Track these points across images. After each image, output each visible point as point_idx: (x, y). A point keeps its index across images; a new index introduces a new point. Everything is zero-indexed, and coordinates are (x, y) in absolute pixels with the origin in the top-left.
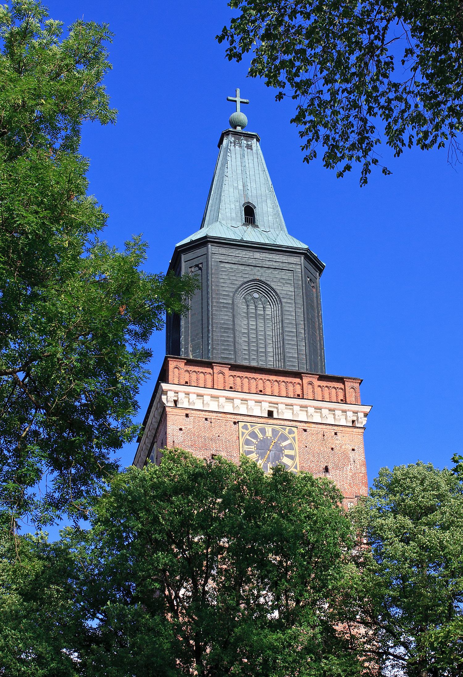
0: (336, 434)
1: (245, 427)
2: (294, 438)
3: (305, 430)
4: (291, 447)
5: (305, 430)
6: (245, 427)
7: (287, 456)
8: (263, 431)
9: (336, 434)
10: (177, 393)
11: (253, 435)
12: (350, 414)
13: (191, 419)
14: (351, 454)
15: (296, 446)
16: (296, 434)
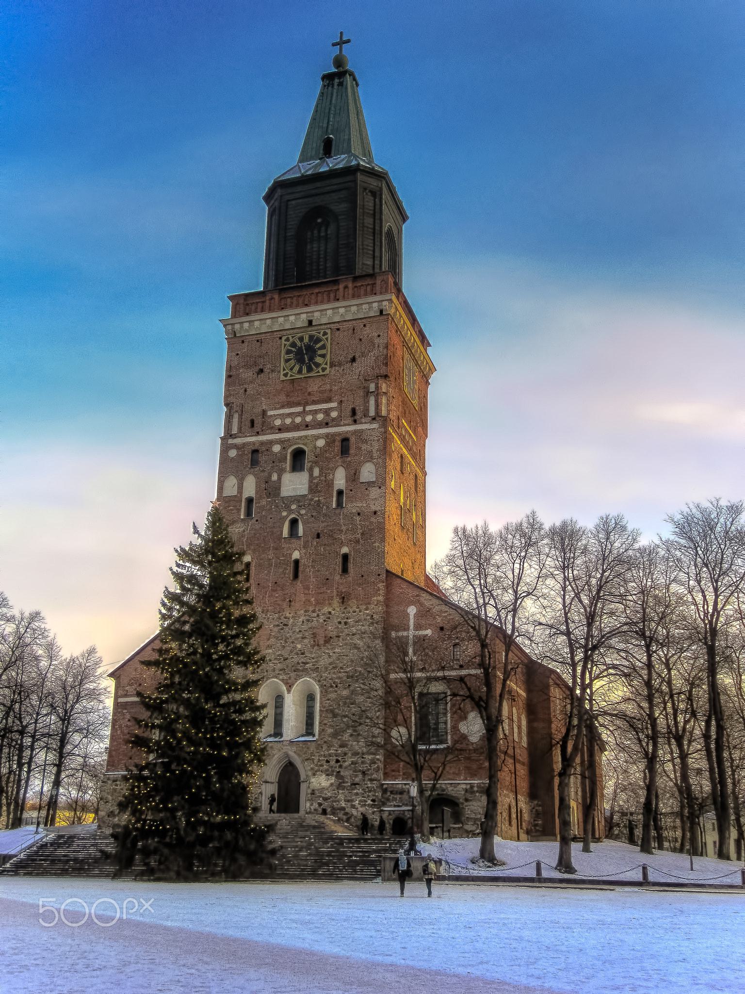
0: (365, 326)
1: (287, 340)
2: (327, 339)
3: (338, 329)
4: (323, 347)
5: (338, 329)
6: (287, 340)
7: (320, 356)
8: (301, 339)
9: (365, 326)
10: (233, 324)
11: (293, 345)
12: (375, 305)
13: (246, 344)
14: (377, 341)
15: (328, 345)
16: (329, 335)
